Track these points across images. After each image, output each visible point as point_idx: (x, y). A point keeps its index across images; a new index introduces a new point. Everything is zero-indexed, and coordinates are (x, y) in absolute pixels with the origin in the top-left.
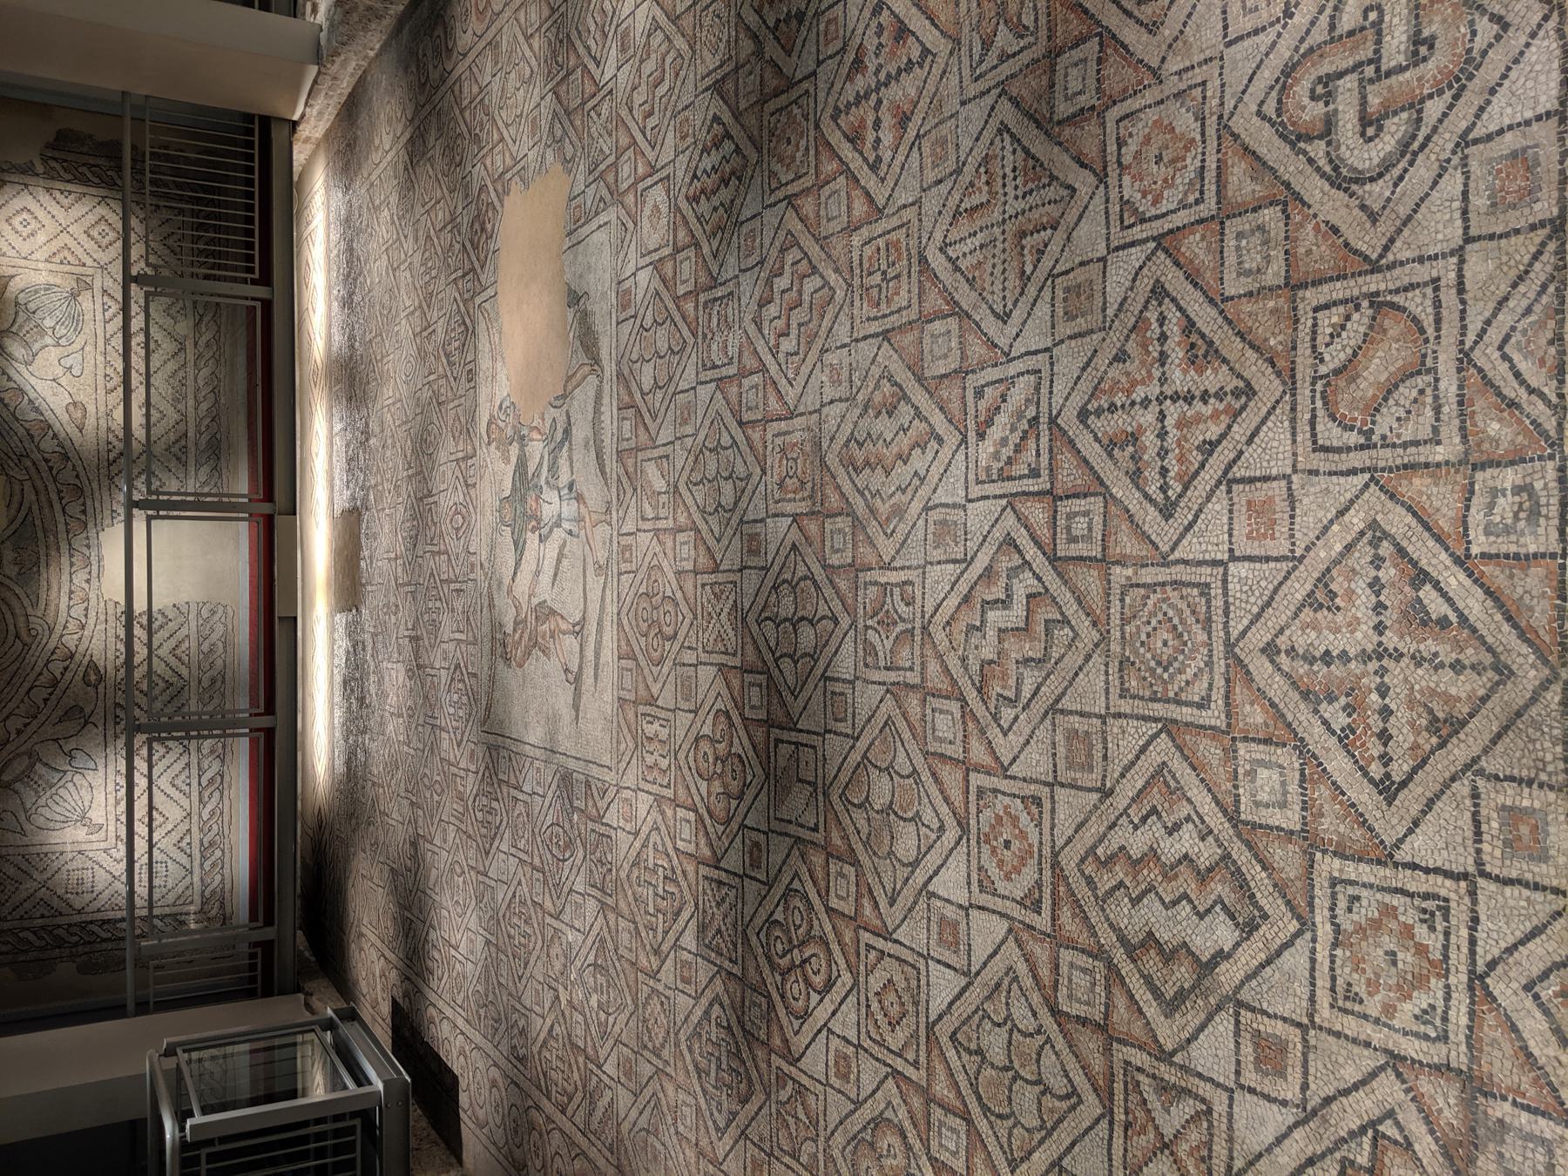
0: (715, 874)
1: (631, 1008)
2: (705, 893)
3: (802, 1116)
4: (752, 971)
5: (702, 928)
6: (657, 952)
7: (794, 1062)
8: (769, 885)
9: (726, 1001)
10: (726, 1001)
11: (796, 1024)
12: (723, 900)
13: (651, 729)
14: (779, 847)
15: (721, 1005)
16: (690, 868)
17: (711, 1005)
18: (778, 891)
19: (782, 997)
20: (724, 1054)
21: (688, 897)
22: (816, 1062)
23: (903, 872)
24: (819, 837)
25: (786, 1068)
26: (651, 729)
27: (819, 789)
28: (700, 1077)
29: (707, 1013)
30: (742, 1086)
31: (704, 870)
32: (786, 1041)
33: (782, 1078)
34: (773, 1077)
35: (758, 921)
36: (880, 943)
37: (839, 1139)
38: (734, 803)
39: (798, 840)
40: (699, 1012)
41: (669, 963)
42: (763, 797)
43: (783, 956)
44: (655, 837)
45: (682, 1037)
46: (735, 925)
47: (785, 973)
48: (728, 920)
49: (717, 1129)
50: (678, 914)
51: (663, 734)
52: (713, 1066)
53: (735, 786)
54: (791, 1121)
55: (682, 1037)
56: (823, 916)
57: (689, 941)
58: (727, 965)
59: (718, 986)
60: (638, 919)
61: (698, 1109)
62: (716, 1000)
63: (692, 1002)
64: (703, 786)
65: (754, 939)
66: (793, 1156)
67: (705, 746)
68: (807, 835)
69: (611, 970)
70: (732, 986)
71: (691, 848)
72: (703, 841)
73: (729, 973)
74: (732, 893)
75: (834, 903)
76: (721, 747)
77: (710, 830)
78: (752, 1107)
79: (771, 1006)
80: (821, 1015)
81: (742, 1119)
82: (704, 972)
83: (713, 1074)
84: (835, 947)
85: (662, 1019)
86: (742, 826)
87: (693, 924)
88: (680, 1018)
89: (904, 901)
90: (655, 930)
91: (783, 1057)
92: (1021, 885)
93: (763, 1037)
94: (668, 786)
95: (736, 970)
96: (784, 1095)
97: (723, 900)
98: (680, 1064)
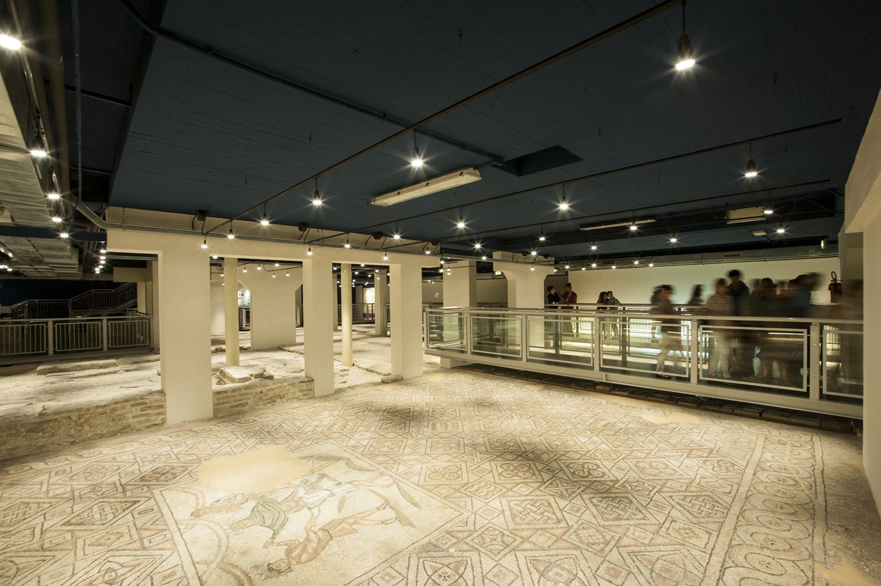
0: (547, 484)
1: (578, 553)
2: (550, 491)
3: (636, 484)
4: (585, 484)
5: (562, 496)
6: (559, 522)
7: (618, 481)
8: (562, 470)
9: (592, 495)
10: (592, 495)
11: (606, 476)
12: (557, 485)
13: (476, 488)
14: (554, 465)
15: (593, 498)
16: (538, 492)
17: (592, 502)
18: (565, 468)
19: (596, 477)
20: (612, 503)
21: (546, 498)
22: (619, 475)
23: (577, 445)
24: (558, 455)
25: (620, 483)
26: (476, 488)
27: (547, 452)
28: (621, 519)
29: (594, 505)
30: (626, 500)
31: (542, 488)
32: (611, 481)
33: (623, 486)
34: (623, 489)
35: (571, 476)
36: (591, 453)
37: (642, 476)
38: (531, 471)
39: (555, 460)
40: (593, 509)
41: (567, 516)
42: (536, 463)
43: (585, 474)
44: (512, 504)
45: (602, 523)
46: (568, 483)
47: (590, 474)
48: (565, 485)
49: (644, 519)
50: (550, 504)
51: (483, 484)
52: (617, 510)
53: (526, 469)
54: (637, 488)
55: (602, 523)
56: (578, 461)
57: (562, 503)
58: (579, 491)
59: (586, 496)
60: (538, 527)
61: (635, 525)
62: (590, 499)
63: (588, 511)
64: (516, 478)
65: (576, 479)
66: (651, 491)
67: (504, 474)
68: (555, 458)
69: (552, 559)
70: (588, 491)
71: (531, 489)
72: (532, 484)
73: (582, 491)
74: (557, 481)
75: (577, 458)
76: (511, 468)
77: (531, 481)
78: (634, 500)
79: (598, 481)
80: (605, 470)
81: (639, 506)
82: (578, 501)
83: (620, 512)
84: (587, 461)
85: (591, 531)
86: (539, 471)
87: (558, 500)
88: (594, 521)
89: (583, 446)
90: (549, 518)
91: (616, 483)
92: (589, 433)
93: (608, 487)
94: (501, 490)
95: (583, 488)
96: (629, 488)
97: (557, 485)
98: (614, 529)
